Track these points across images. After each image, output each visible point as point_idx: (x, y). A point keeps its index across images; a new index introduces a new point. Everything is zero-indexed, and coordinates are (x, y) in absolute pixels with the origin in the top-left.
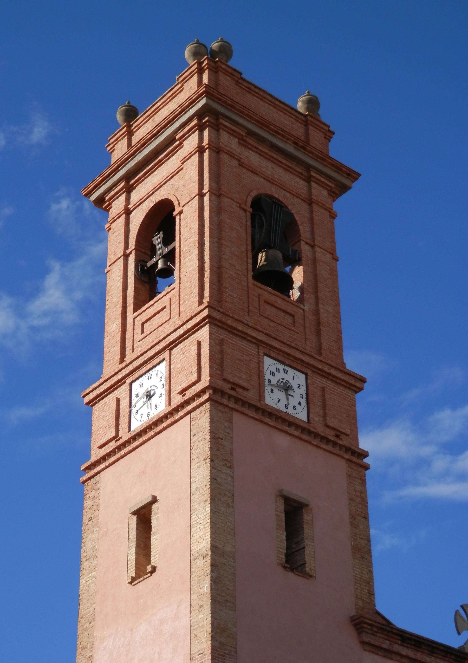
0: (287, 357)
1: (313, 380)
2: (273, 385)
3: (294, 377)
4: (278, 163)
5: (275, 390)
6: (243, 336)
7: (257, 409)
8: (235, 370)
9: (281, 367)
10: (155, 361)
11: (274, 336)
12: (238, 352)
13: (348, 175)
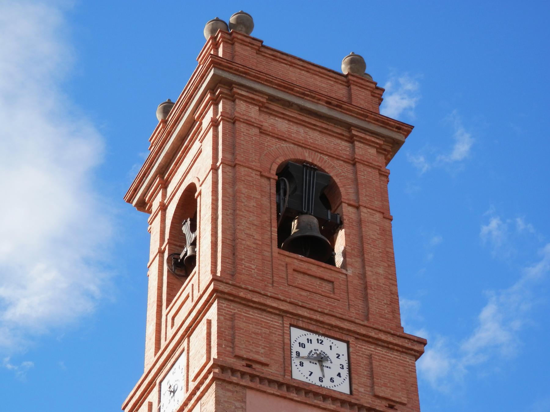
0: (321, 325)
1: (357, 348)
2: (303, 358)
3: (331, 347)
4: (313, 127)
5: (306, 363)
6: (262, 308)
7: (280, 385)
8: (250, 345)
9: (314, 337)
10: (177, 353)
11: (300, 304)
12: (254, 326)
13: (399, 128)
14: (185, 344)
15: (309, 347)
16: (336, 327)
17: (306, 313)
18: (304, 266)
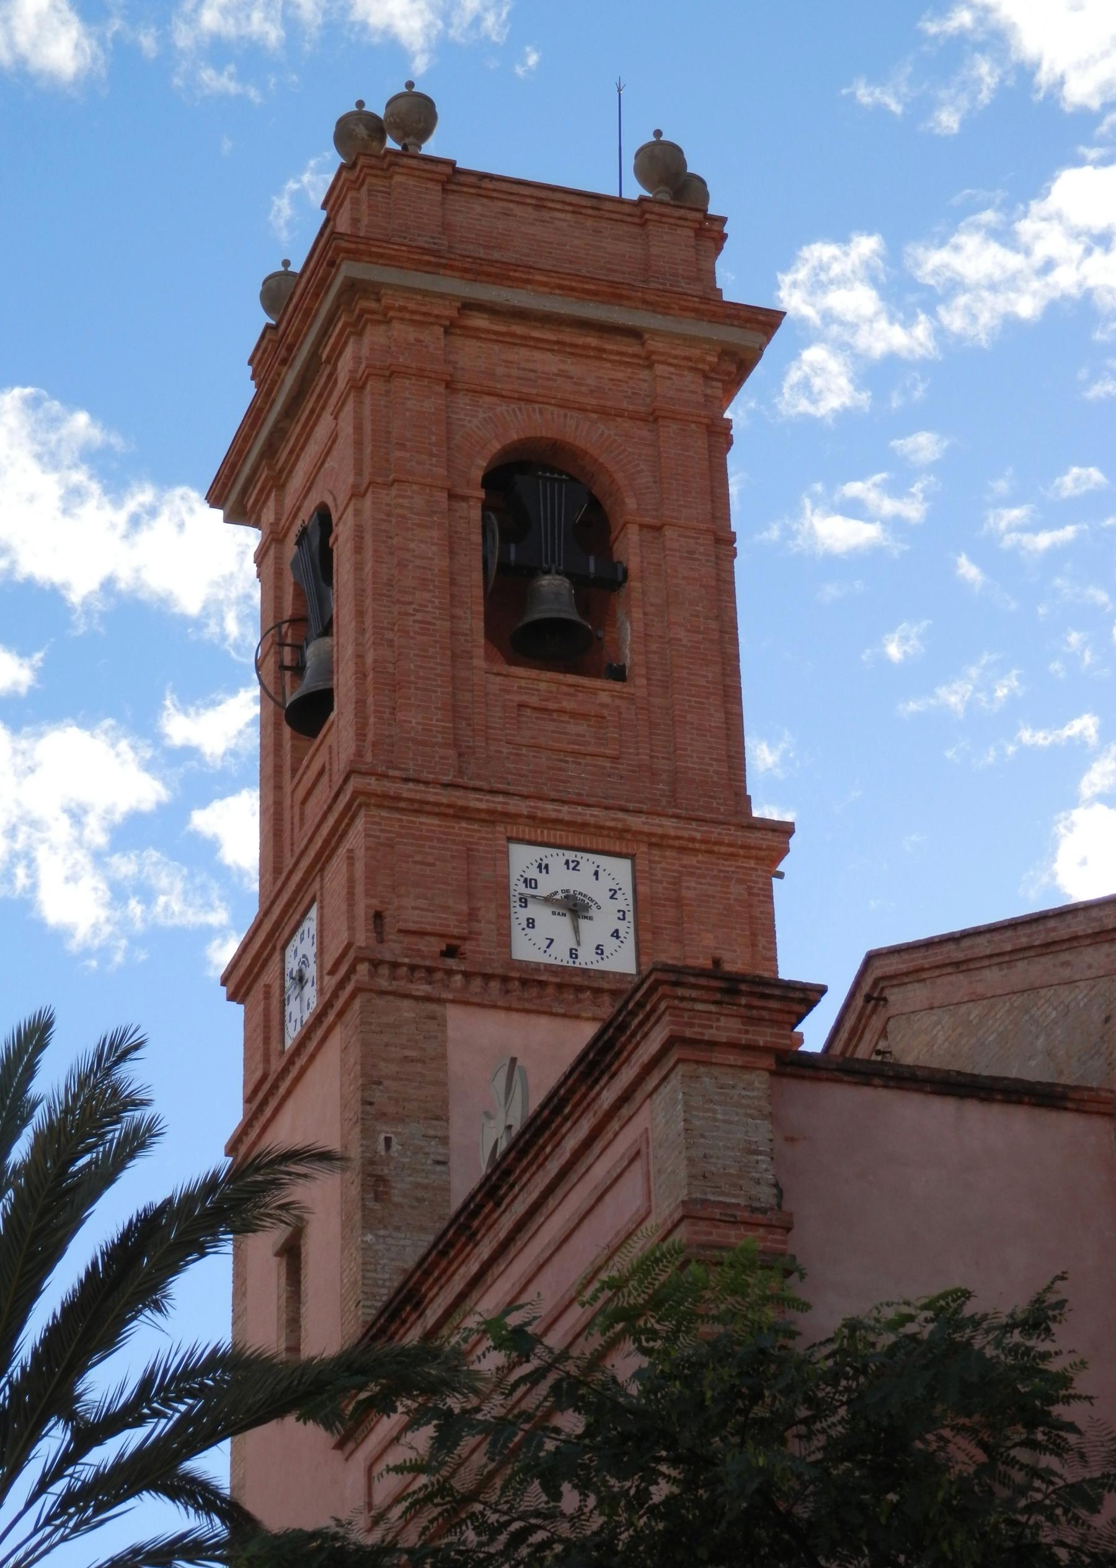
14: (316, 886)
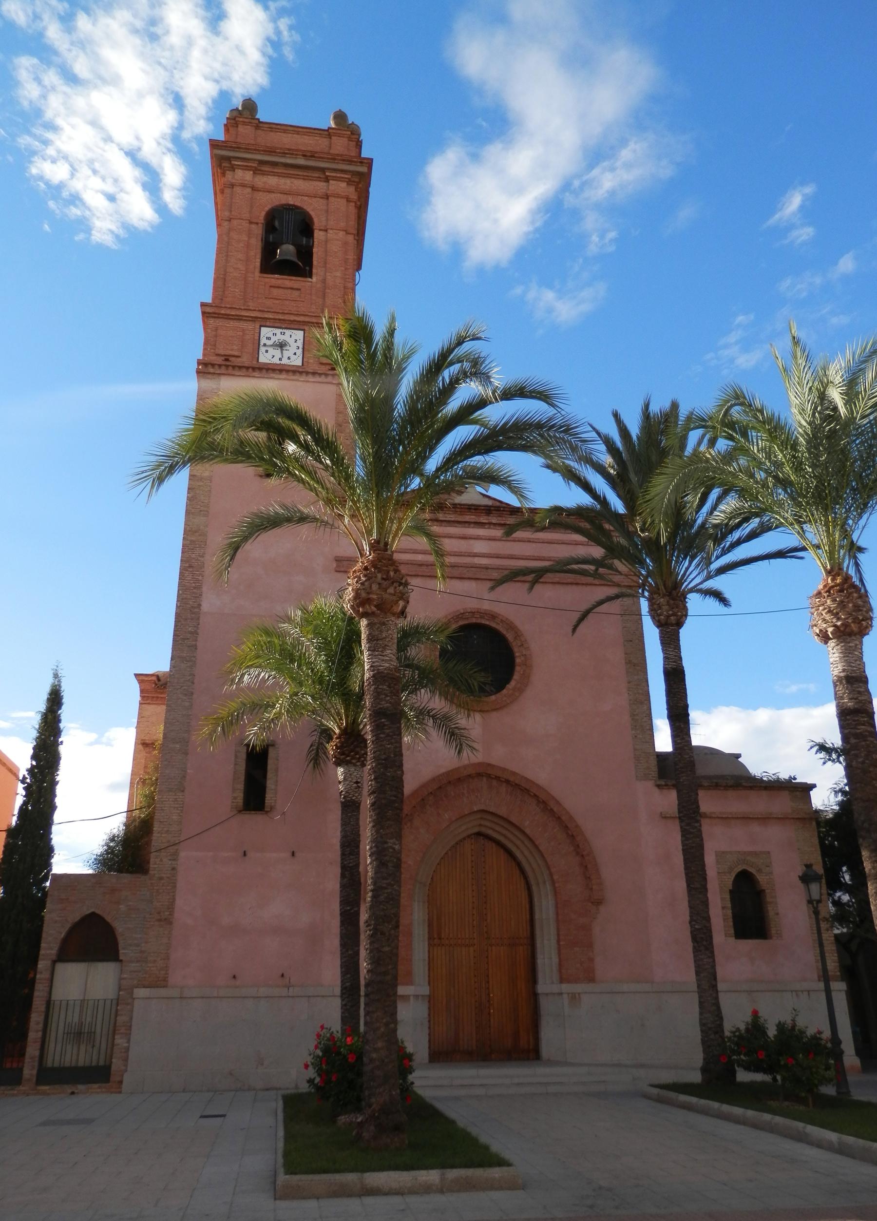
4: (297, 177)
5: (270, 350)
15: (274, 339)
16: (295, 321)
17: (271, 316)
18: (279, 282)
